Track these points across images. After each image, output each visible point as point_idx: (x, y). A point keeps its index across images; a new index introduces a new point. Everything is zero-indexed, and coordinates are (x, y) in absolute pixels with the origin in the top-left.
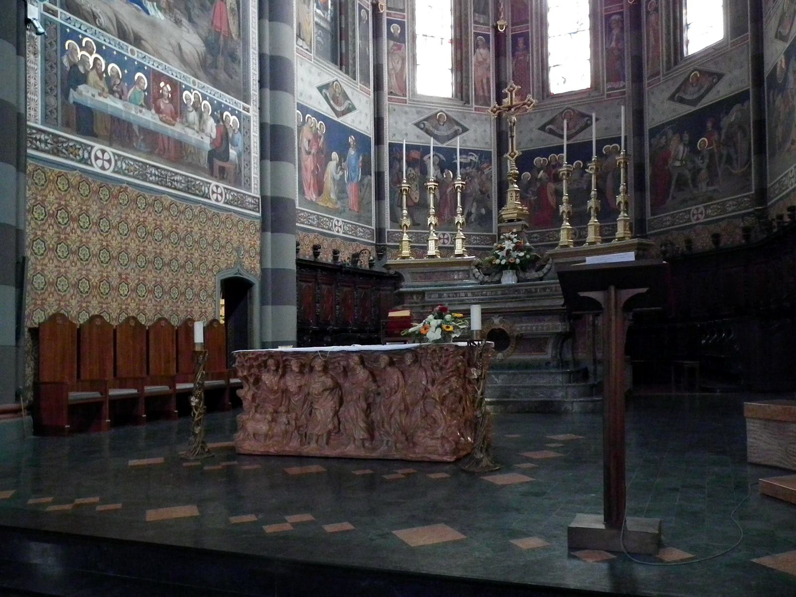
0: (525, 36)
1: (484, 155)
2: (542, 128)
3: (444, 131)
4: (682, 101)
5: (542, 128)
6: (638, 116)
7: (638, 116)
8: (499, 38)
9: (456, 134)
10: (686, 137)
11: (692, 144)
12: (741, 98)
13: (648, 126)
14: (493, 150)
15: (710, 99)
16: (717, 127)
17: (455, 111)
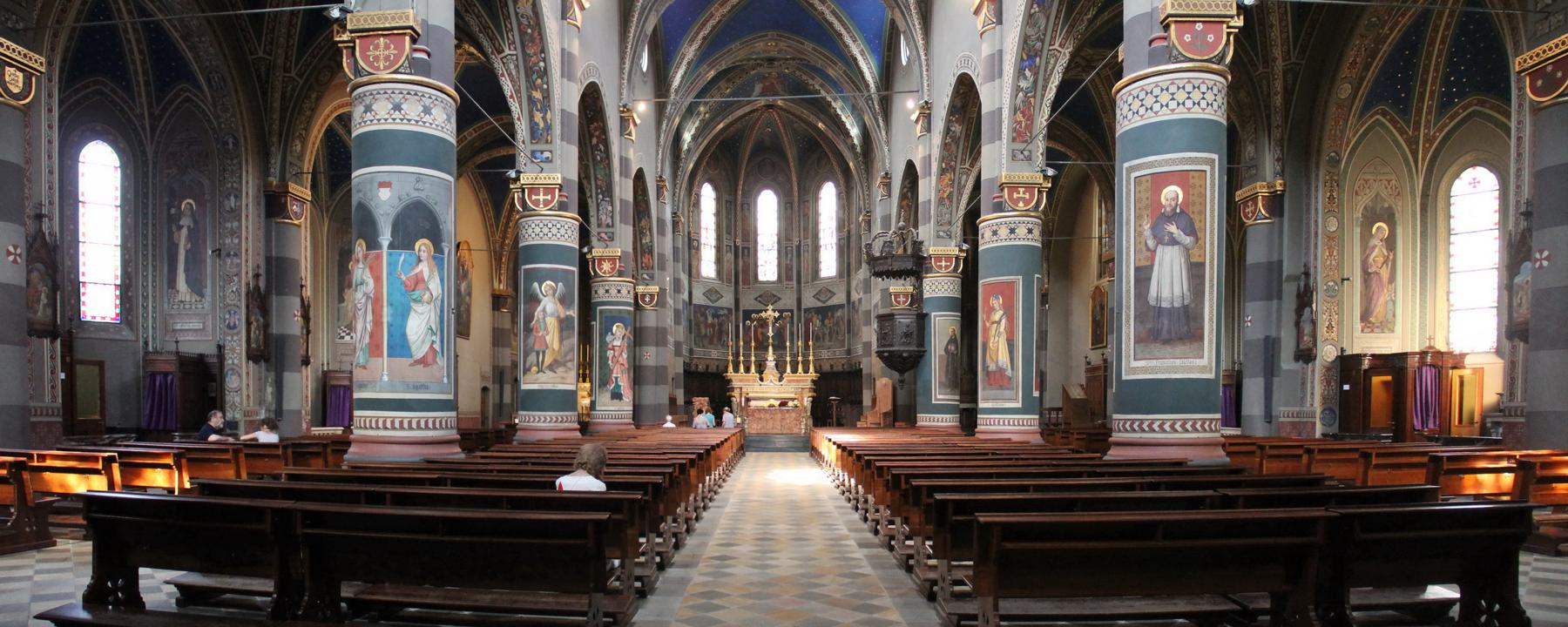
0: (748, 249)
1: (729, 310)
2: (756, 299)
3: (714, 298)
4: (818, 299)
5: (756, 299)
6: (799, 301)
7: (799, 301)
8: (736, 248)
9: (718, 299)
10: (820, 317)
11: (822, 321)
12: (842, 306)
13: (803, 307)
14: (733, 307)
15: (830, 303)
16: (833, 316)
17: (717, 284)
